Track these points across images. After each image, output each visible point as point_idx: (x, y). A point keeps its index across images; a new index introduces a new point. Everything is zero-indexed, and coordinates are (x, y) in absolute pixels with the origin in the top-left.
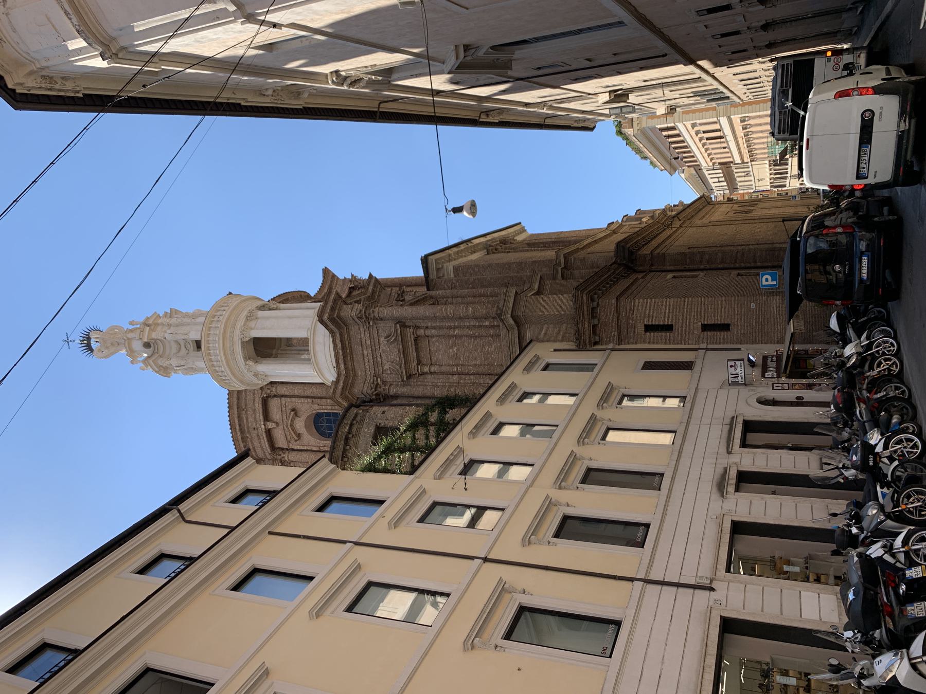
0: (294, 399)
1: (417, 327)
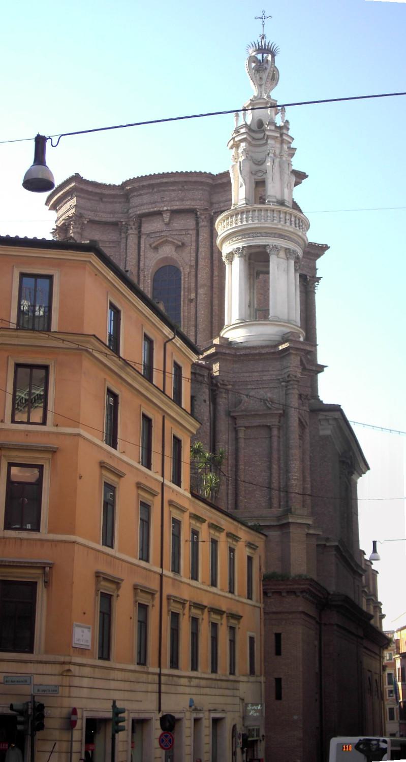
0: (194, 244)
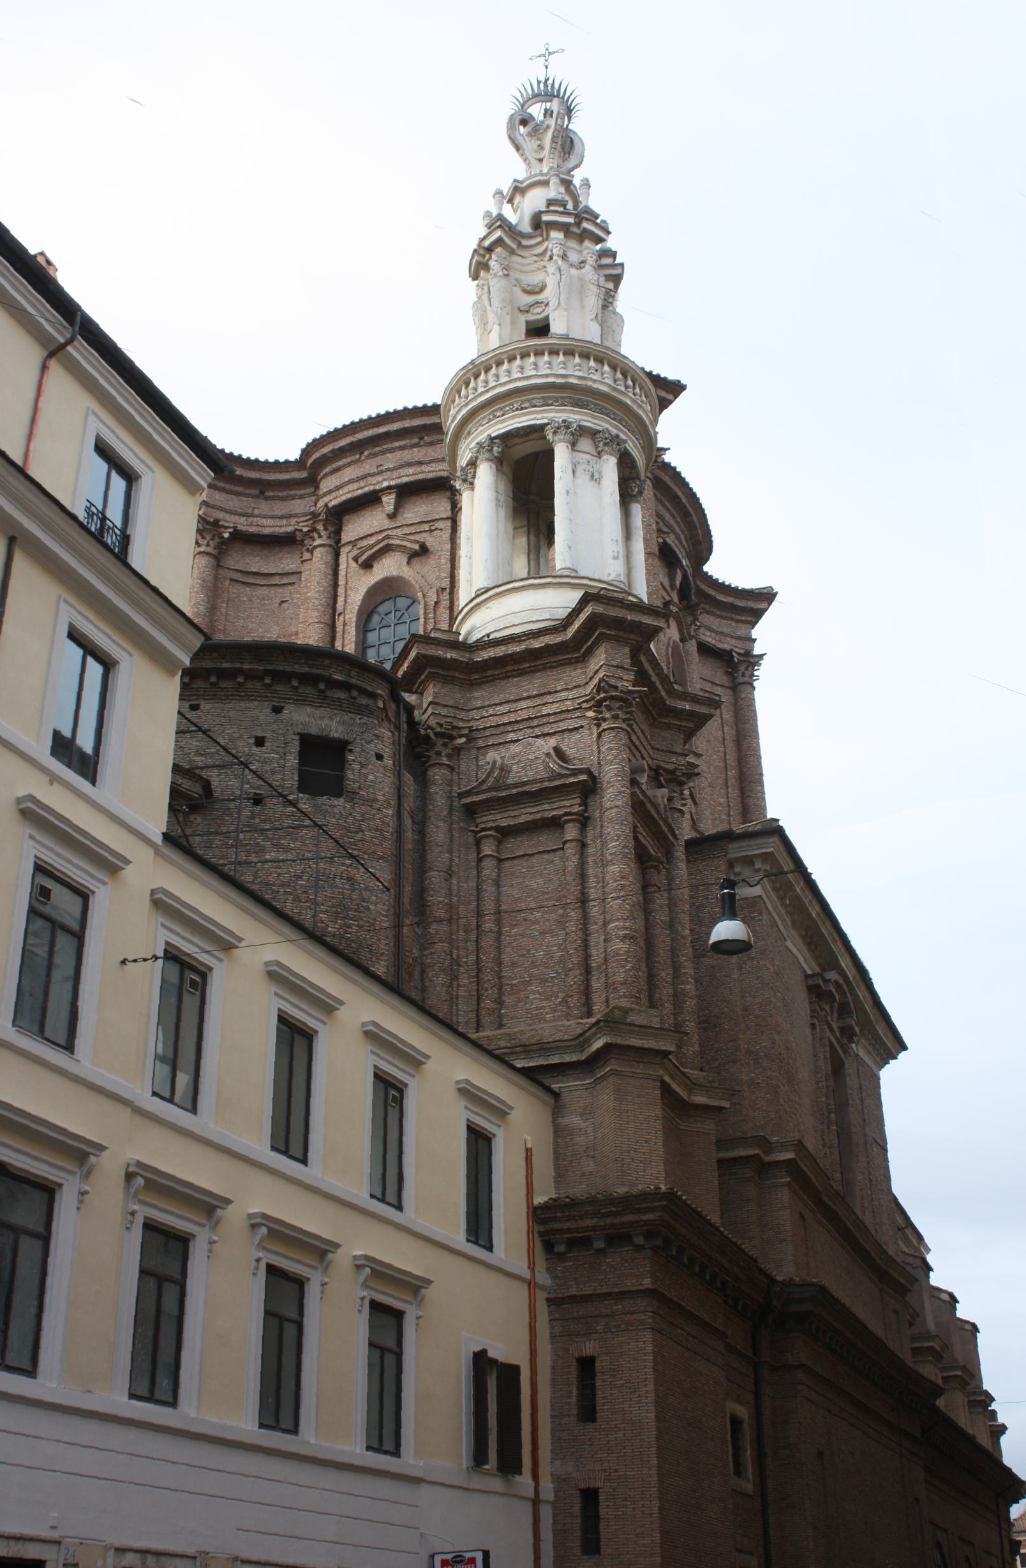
0: (448, 547)
1: (584, 821)
